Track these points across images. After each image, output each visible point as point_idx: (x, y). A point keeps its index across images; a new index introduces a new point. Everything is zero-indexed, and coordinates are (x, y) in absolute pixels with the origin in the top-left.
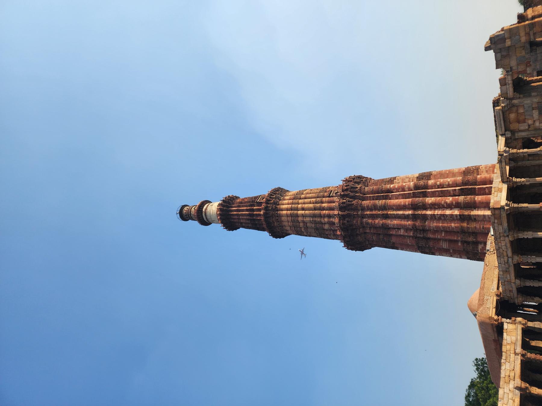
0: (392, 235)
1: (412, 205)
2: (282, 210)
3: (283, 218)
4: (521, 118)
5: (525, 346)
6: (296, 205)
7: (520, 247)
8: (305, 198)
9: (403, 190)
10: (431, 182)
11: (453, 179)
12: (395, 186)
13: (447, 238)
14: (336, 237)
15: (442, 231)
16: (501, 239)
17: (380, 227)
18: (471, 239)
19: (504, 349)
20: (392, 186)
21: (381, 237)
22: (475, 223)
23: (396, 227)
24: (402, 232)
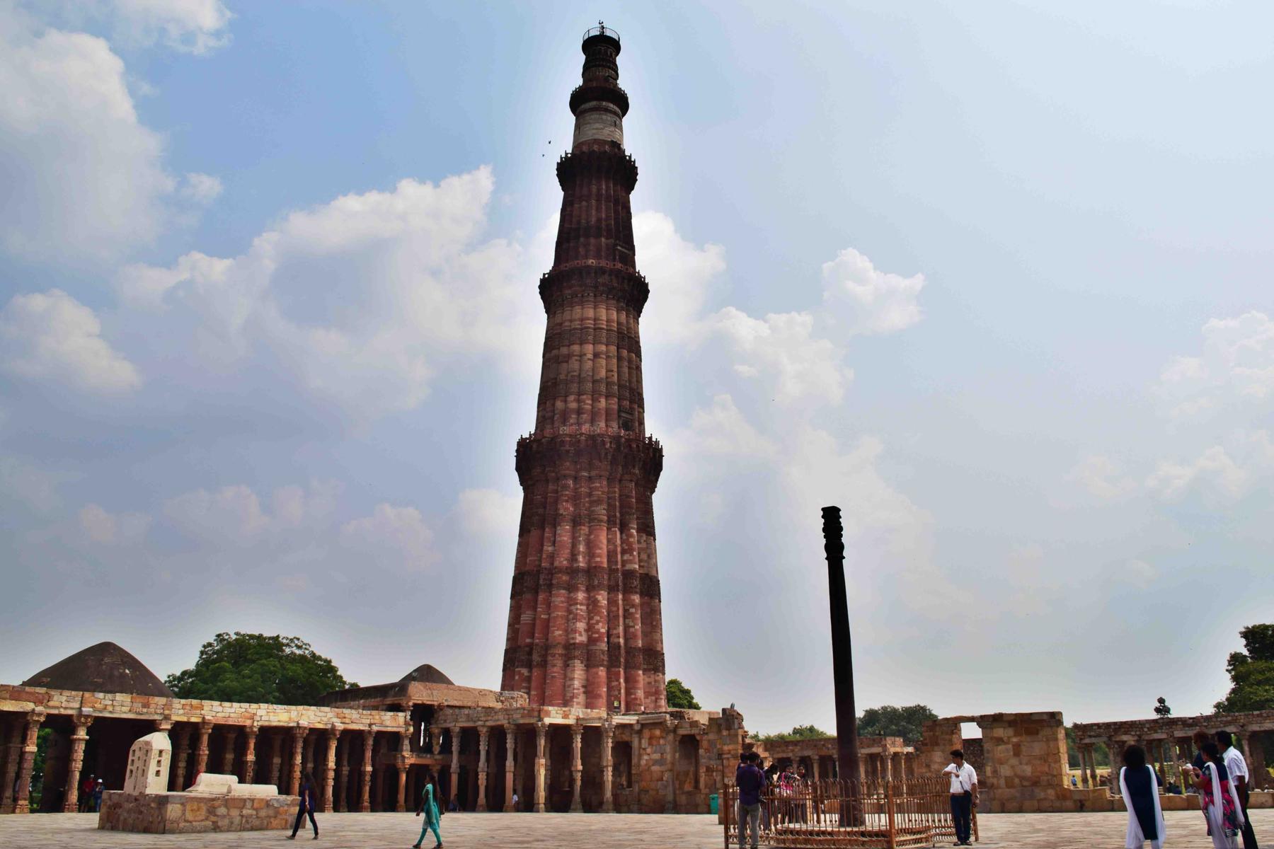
0: (543, 529)
2: (595, 308)
3: (578, 309)
4: (654, 742)
5: (380, 735)
6: (604, 340)
7: (498, 734)
8: (620, 358)
9: (624, 552)
10: (636, 599)
11: (639, 634)
12: (632, 535)
14: (541, 421)
17: (557, 509)
18: (536, 657)
19: (374, 712)
20: (634, 532)
21: (541, 511)
23: (558, 539)
24: (548, 548)
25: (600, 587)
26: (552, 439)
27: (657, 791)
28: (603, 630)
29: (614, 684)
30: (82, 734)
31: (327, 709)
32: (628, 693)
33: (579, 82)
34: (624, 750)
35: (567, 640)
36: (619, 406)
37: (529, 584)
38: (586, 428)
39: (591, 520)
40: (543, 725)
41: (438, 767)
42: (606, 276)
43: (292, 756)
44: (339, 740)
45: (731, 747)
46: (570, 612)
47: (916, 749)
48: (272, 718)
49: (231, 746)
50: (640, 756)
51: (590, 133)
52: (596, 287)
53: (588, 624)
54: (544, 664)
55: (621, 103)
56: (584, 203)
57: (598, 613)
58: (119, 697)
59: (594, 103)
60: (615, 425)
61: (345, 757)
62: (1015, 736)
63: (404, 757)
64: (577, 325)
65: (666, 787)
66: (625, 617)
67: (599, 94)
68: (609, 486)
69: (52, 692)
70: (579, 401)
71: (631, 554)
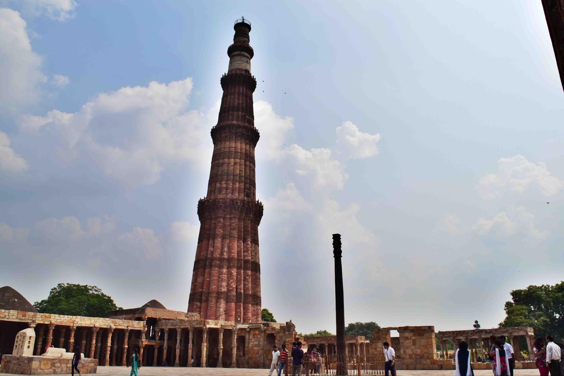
0: (209, 241)
3: (228, 143)
4: (255, 336)
7: (185, 332)
8: (245, 166)
9: (244, 252)
10: (249, 272)
11: (250, 288)
13: (205, 281)
14: (210, 192)
17: (215, 232)
18: (204, 298)
19: (130, 321)
20: (249, 243)
21: (208, 232)
24: (211, 249)
25: (233, 267)
27: (256, 358)
28: (234, 286)
29: (239, 310)
31: (108, 319)
32: (244, 314)
33: (232, 42)
34: (242, 340)
35: (218, 290)
36: (245, 186)
37: (202, 264)
38: (229, 196)
39: (230, 237)
40: (206, 328)
41: (158, 346)
42: (241, 129)
43: (91, 340)
44: (113, 333)
45: (289, 339)
46: (219, 277)
47: (371, 341)
48: (82, 323)
49: (63, 335)
50: (249, 343)
51: (236, 65)
52: (236, 134)
54: (207, 301)
55: (251, 53)
57: (233, 279)
58: (12, 311)
59: (238, 52)
60: (242, 195)
61: (116, 341)
62: (414, 336)
63: (142, 342)
64: (227, 150)
65: (260, 357)
66: (244, 281)
67: (241, 48)
68: (239, 222)
70: (227, 184)
71: (248, 253)
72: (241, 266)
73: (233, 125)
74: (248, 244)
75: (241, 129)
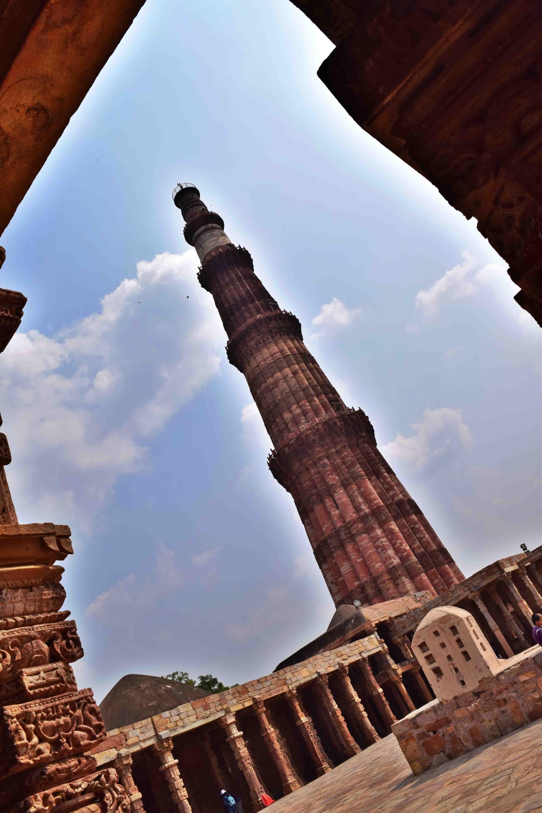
1: (377, 508)
2: (276, 344)
6: (295, 362)
8: (310, 369)
15: (363, 557)
16: (466, 589)
18: (370, 591)
19: (357, 642)
21: (314, 491)
22: (393, 586)
26: (297, 438)
29: (436, 581)
30: (170, 760)
31: (327, 653)
33: (183, 224)
42: (273, 321)
51: (211, 245)
52: (270, 331)
53: (394, 549)
56: (231, 286)
57: (398, 538)
58: (182, 708)
59: (203, 228)
64: (270, 360)
66: (415, 534)
69: (126, 730)
70: (300, 407)
71: (394, 490)
72: (398, 514)
73: (258, 320)
74: (385, 478)
75: (273, 321)
